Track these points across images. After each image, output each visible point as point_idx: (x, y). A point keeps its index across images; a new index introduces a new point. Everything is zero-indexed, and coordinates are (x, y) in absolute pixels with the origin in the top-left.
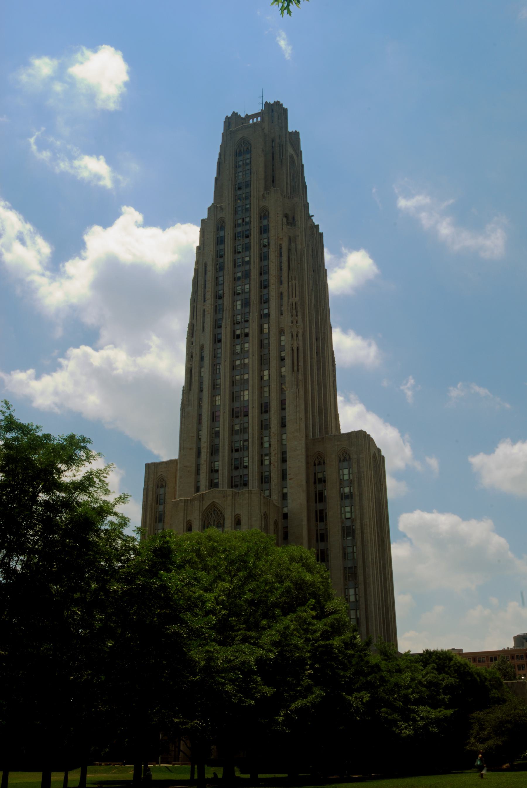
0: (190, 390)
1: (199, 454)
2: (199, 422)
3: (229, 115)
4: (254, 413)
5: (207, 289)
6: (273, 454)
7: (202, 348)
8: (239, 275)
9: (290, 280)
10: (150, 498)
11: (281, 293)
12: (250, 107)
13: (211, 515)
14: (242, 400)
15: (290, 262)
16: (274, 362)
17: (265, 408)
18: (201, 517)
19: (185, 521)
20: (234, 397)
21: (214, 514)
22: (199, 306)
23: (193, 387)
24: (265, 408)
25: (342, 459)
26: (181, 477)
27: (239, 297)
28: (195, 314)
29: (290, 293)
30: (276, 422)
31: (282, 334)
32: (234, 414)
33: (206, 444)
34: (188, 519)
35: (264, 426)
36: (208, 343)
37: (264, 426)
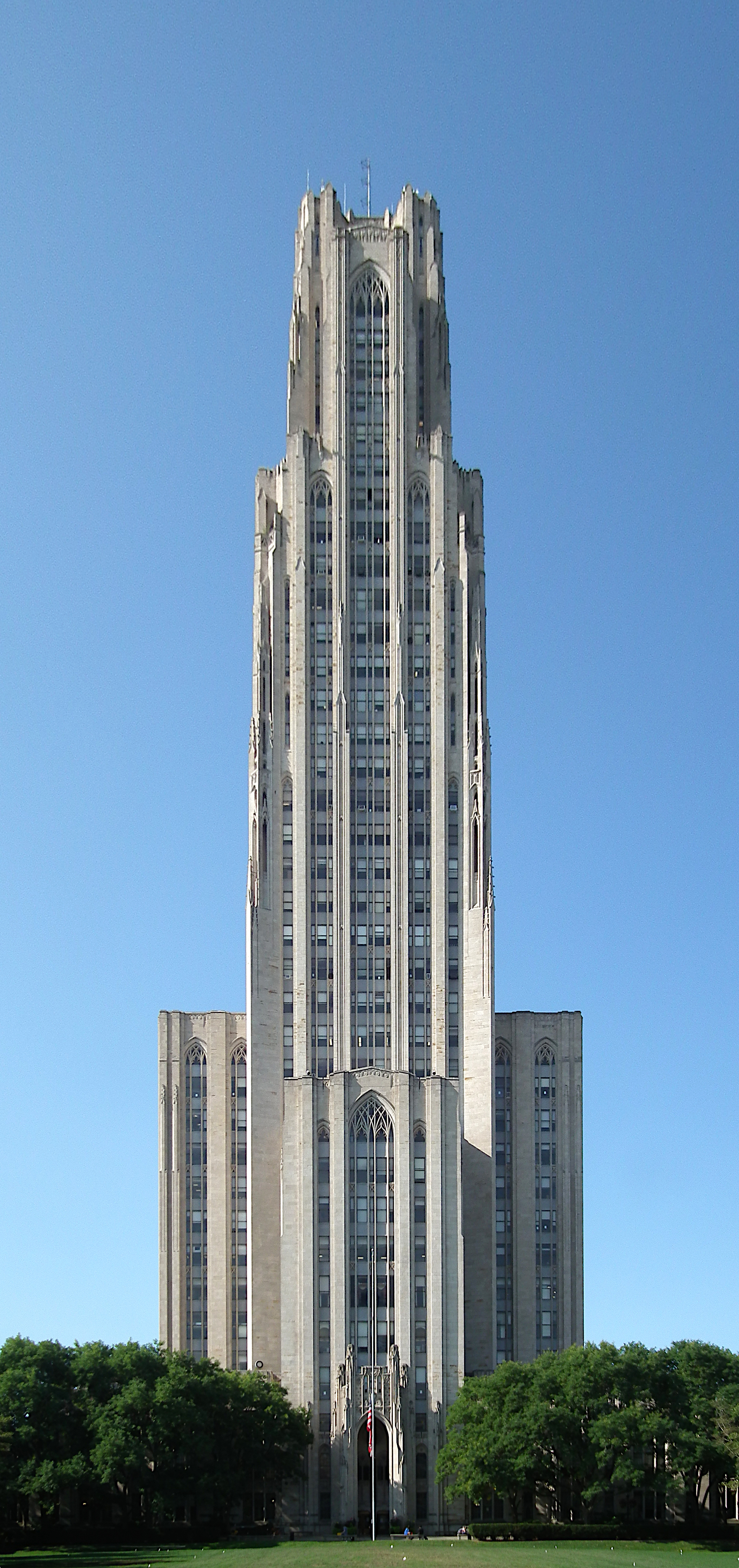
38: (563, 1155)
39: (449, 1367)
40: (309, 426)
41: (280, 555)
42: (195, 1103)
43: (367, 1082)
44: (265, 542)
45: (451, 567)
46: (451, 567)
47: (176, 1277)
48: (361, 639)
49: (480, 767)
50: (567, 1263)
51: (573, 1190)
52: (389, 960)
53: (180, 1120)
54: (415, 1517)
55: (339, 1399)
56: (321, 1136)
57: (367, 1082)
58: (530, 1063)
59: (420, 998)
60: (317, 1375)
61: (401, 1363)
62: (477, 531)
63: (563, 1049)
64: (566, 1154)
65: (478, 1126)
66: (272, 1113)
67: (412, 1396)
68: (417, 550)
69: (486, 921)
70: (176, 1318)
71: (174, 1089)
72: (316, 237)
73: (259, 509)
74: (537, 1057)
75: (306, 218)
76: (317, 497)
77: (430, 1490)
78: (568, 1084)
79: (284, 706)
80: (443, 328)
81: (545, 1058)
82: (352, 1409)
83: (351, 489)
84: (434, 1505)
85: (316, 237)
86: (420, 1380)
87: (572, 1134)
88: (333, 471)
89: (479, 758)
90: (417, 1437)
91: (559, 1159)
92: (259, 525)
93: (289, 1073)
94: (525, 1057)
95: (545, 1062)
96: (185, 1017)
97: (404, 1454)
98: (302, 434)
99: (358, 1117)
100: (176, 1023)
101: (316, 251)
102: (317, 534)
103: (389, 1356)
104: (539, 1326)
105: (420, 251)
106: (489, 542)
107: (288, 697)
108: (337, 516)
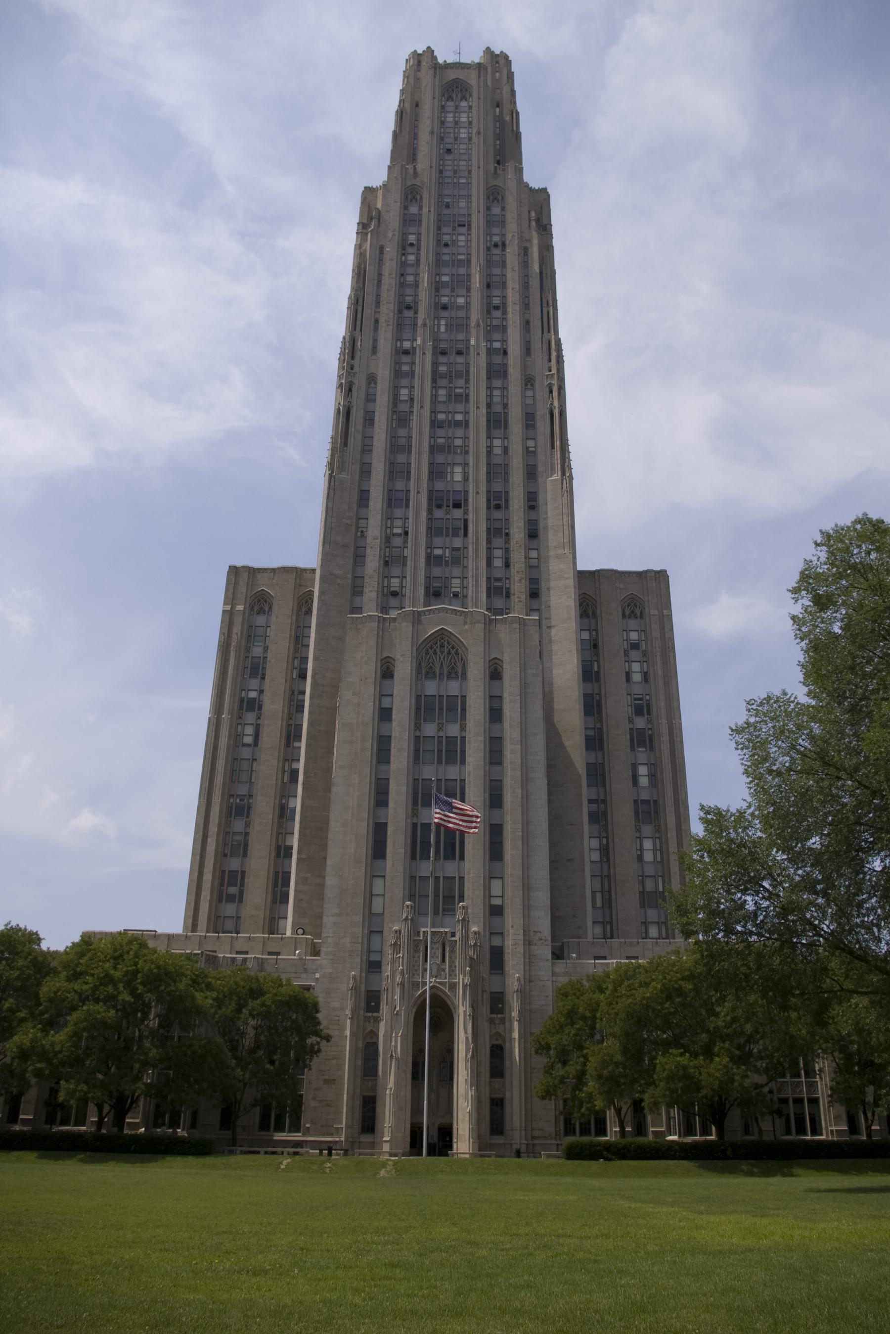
0: (346, 445)
1: (359, 557)
3: (420, 51)
4: (477, 503)
5: (384, 287)
6: (517, 579)
7: (372, 379)
8: (445, 279)
9: (545, 304)
10: (237, 629)
11: (528, 322)
12: (457, 48)
13: (435, 653)
14: (449, 479)
15: (544, 279)
16: (516, 427)
17: (497, 502)
18: (414, 654)
19: (379, 658)
20: (436, 472)
21: (442, 653)
22: (367, 311)
23: (351, 440)
24: (497, 502)
25: (627, 613)
26: (322, 593)
27: (445, 314)
28: (359, 323)
29: (545, 325)
30: (522, 524)
31: (529, 387)
32: (436, 501)
33: (378, 541)
34: (385, 655)
36: (387, 372)
37: (498, 531)
39: (532, 934)
47: (213, 829)
49: (554, 371)
50: (671, 820)
52: (466, 521)
53: (236, 667)
54: (488, 1132)
55: (393, 972)
60: (365, 940)
62: (545, 222)
64: (662, 704)
69: (565, 488)
70: (208, 877)
71: (234, 636)
77: (508, 1094)
78: (658, 635)
79: (372, 328)
82: (410, 985)
90: (491, 1021)
91: (654, 709)
98: (399, 165)
99: (427, 653)
107: (377, 321)
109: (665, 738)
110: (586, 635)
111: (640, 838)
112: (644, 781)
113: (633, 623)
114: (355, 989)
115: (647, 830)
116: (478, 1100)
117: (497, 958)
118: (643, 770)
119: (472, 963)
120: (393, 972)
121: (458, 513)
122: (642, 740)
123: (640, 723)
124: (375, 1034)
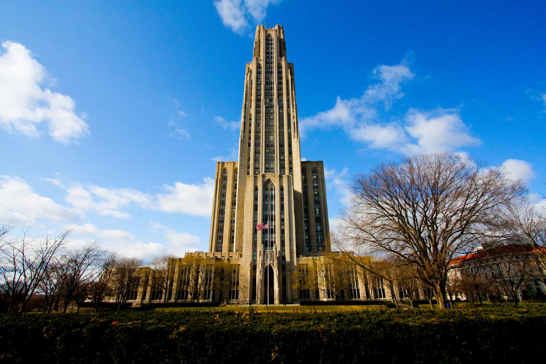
2: (249, 145)
7: (250, 115)
35: (282, 153)
38: (321, 194)
40: (257, 56)
41: (250, 76)
42: (224, 182)
43: (269, 176)
44: (247, 74)
45: (287, 78)
46: (287, 78)
47: (215, 226)
48: (268, 90)
50: (324, 222)
51: (324, 203)
56: (256, 189)
57: (269, 176)
58: (311, 172)
59: (282, 158)
61: (278, 250)
63: (319, 169)
65: (298, 186)
66: (244, 183)
67: (281, 259)
68: (280, 70)
72: (259, 31)
73: (247, 69)
74: (312, 171)
75: (258, 28)
76: (259, 67)
80: (284, 43)
81: (314, 171)
82: (263, 264)
83: (266, 66)
84: (289, 294)
85: (259, 31)
86: (283, 255)
87: (323, 189)
88: (262, 63)
89: (295, 110)
90: (282, 272)
92: (247, 71)
93: (248, 174)
94: (309, 172)
95: (315, 172)
96: (223, 163)
97: (279, 277)
100: (221, 164)
101: (259, 33)
102: (259, 73)
103: (274, 247)
104: (317, 240)
105: (280, 33)
106: (295, 74)
108: (263, 70)
109: (323, 202)
110: (303, 177)
111: (317, 226)
112: (317, 213)
113: (315, 174)
114: (251, 264)
115: (318, 224)
116: (280, 290)
117: (284, 258)
118: (317, 210)
119: (278, 258)
120: (259, 259)
121: (272, 148)
122: (317, 202)
123: (317, 198)
124: (255, 275)
